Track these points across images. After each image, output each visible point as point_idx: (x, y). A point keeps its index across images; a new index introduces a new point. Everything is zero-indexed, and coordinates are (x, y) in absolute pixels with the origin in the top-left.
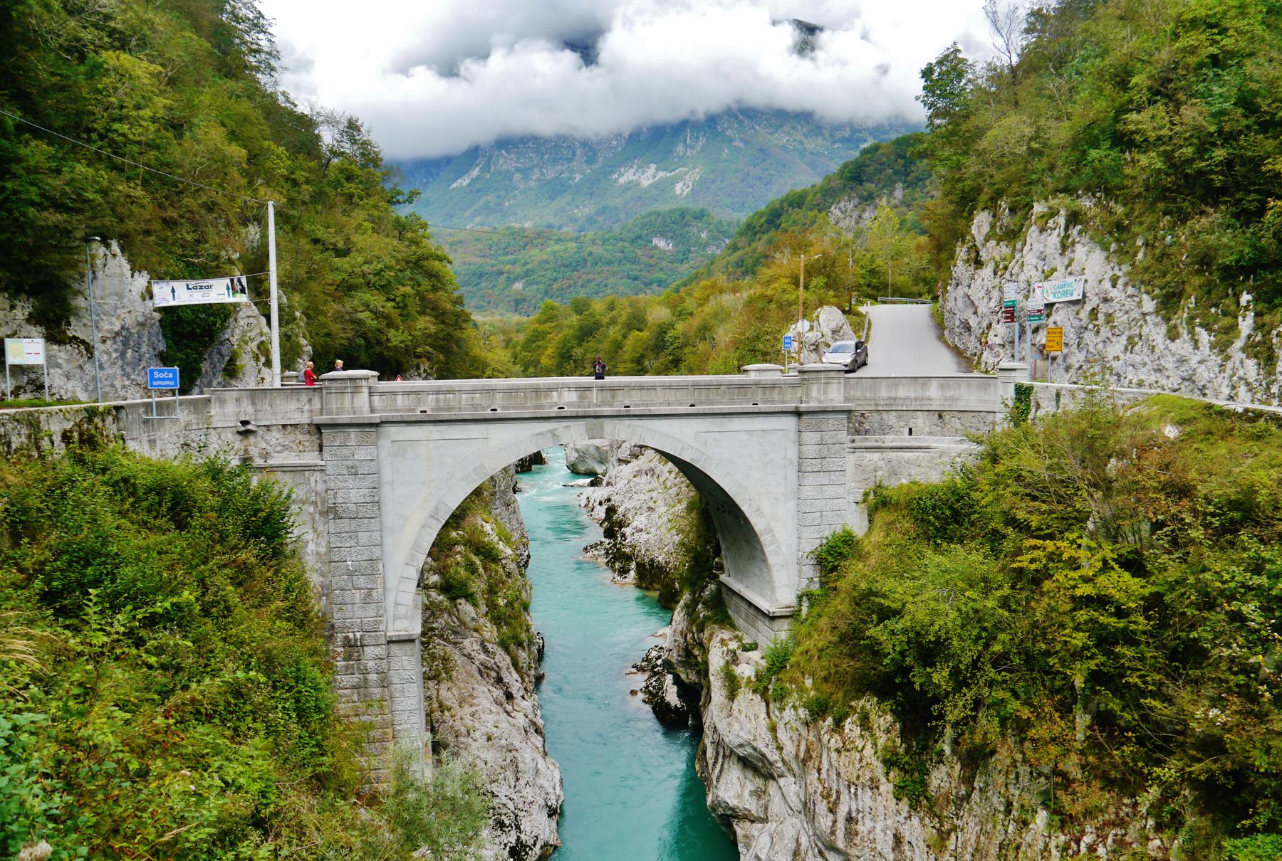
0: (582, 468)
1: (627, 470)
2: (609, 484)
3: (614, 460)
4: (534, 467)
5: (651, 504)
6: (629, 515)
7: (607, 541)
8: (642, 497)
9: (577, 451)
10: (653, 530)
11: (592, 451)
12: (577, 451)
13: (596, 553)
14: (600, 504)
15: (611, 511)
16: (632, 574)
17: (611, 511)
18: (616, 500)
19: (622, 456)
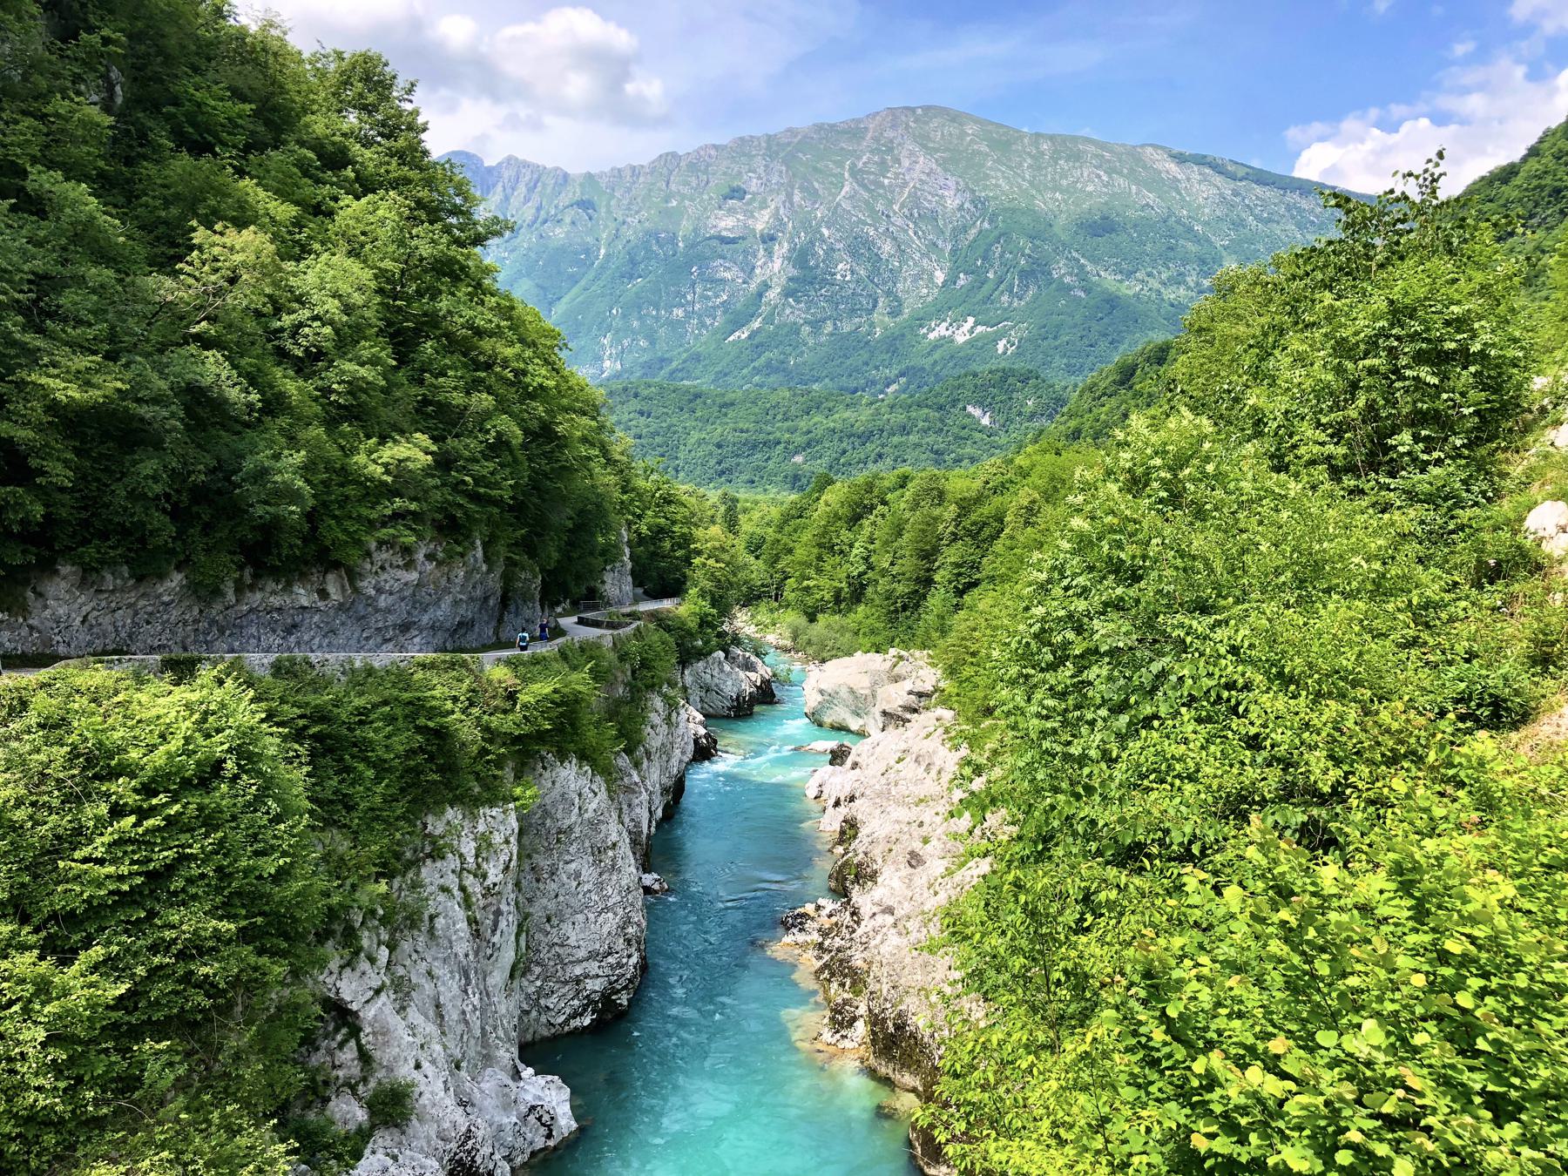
0: (827, 720)
1: (893, 740)
2: (855, 765)
3: (877, 711)
4: (756, 709)
5: (917, 845)
6: (877, 852)
7: (829, 905)
8: (903, 814)
9: (821, 692)
10: (912, 925)
11: (844, 693)
12: (821, 692)
13: (801, 938)
14: (837, 804)
15: (850, 829)
16: (861, 1028)
17: (850, 829)
18: (860, 809)
19: (894, 706)
